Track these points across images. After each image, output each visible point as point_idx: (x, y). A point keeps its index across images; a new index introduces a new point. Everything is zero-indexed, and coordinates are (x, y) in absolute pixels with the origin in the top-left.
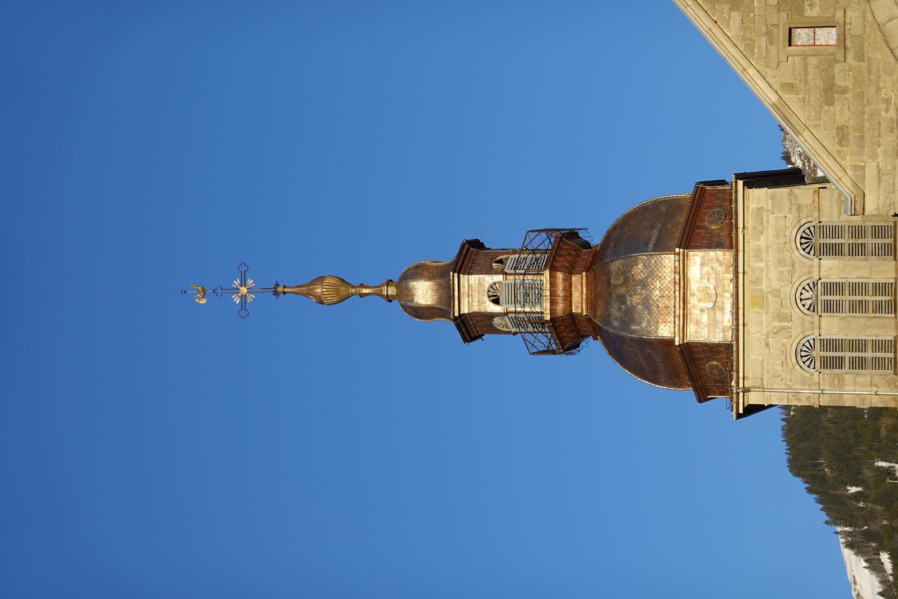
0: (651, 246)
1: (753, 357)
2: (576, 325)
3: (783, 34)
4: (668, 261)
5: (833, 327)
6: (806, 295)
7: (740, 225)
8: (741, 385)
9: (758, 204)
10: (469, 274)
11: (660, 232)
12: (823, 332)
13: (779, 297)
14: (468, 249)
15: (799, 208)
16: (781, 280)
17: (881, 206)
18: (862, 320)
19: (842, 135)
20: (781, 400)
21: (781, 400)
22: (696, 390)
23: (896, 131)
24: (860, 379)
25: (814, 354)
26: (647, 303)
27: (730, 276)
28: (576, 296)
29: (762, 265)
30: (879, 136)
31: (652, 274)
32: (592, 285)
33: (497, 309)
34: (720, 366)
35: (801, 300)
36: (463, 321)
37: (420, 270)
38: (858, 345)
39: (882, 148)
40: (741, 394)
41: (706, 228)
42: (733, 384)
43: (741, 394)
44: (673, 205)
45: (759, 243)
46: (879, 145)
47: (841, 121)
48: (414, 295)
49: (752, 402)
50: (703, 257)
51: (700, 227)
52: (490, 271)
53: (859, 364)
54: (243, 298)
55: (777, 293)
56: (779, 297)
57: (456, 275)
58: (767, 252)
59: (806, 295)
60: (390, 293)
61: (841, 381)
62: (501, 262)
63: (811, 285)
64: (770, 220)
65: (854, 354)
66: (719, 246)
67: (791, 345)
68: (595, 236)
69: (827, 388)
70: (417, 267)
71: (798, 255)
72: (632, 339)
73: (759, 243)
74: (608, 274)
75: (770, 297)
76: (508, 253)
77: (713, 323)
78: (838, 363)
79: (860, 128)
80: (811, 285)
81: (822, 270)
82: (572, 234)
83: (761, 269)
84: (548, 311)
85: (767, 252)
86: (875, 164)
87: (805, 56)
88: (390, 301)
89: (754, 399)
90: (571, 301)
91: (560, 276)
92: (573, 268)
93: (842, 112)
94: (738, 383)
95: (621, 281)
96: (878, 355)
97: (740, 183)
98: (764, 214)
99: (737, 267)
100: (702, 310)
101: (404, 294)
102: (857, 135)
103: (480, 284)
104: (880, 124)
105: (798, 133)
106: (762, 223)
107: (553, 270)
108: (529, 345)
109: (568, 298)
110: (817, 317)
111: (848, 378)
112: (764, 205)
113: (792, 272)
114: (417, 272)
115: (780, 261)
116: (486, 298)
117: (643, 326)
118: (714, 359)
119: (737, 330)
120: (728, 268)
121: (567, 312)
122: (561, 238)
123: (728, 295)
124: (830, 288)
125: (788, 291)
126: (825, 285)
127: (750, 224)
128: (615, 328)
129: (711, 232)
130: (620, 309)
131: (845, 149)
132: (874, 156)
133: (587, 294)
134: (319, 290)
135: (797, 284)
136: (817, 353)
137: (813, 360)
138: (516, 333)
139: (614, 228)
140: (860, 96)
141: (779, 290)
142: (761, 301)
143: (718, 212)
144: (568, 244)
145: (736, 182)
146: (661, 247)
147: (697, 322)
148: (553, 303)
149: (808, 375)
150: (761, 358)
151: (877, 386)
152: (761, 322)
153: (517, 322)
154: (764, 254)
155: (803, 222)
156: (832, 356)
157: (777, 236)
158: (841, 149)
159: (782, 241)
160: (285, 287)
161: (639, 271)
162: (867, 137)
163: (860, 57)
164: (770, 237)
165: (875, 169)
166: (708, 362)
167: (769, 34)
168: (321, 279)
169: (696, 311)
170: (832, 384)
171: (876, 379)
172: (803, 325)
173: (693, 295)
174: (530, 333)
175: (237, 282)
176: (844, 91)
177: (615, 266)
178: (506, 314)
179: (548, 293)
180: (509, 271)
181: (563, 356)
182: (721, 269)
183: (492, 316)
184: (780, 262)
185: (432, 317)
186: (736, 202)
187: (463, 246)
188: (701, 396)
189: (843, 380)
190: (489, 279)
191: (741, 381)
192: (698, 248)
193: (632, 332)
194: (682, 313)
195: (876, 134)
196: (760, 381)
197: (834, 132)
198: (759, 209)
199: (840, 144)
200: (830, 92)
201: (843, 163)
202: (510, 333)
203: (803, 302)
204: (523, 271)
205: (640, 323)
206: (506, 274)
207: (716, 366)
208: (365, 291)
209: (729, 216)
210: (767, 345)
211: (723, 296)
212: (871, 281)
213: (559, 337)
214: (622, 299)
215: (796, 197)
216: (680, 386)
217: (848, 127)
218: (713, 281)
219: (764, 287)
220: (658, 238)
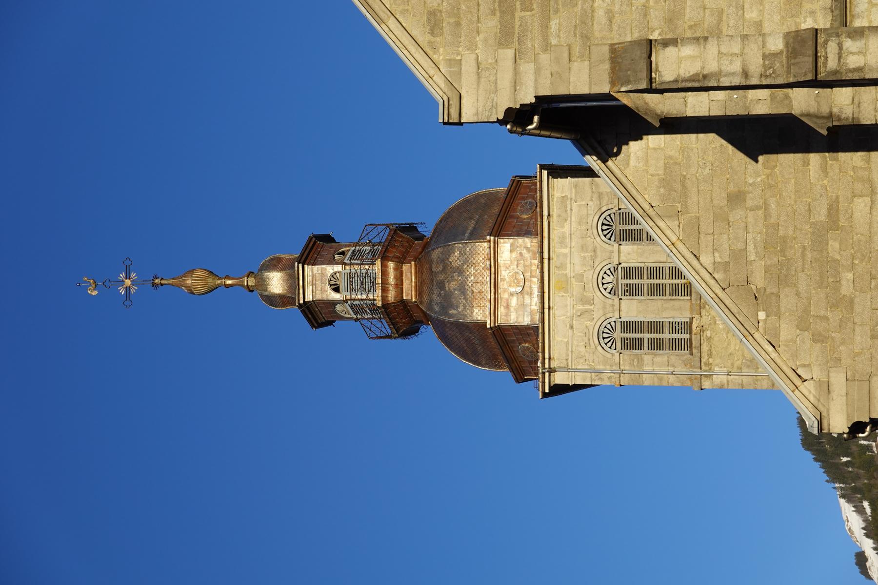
0: (467, 235)
1: (559, 339)
2: (408, 311)
4: (483, 247)
5: (633, 309)
6: (607, 279)
7: (545, 213)
8: (547, 366)
9: (562, 192)
10: (313, 264)
11: (477, 223)
12: (623, 314)
13: (582, 281)
14: (315, 243)
15: (600, 196)
16: (584, 265)
17: (480, 109)
18: (660, 303)
20: (584, 380)
21: (584, 380)
22: (512, 370)
23: (498, 14)
24: (658, 359)
25: (615, 335)
27: (536, 262)
28: (406, 285)
29: (566, 251)
30: (478, 21)
32: (419, 272)
33: (336, 296)
34: (532, 348)
35: (603, 284)
36: (308, 308)
37: (274, 262)
38: (656, 327)
39: (482, 36)
40: (547, 374)
41: (518, 217)
42: (539, 364)
43: (547, 374)
44: (491, 197)
45: (564, 230)
46: (478, 33)
48: (267, 285)
49: (557, 382)
50: (512, 245)
51: (512, 217)
52: (332, 262)
53: (657, 345)
54: (128, 289)
55: (580, 277)
56: (582, 281)
57: (300, 265)
58: (571, 238)
59: (607, 279)
60: (250, 284)
61: (641, 361)
62: (343, 253)
63: (612, 269)
64: (574, 208)
65: (653, 336)
66: (527, 233)
67: (593, 326)
68: (427, 230)
69: (627, 368)
70: (272, 260)
71: (599, 241)
72: (451, 323)
73: (564, 230)
74: (430, 262)
75: (573, 282)
76: (350, 246)
77: (523, 306)
78: (637, 344)
79: (455, 12)
80: (612, 269)
81: (622, 255)
82: (411, 229)
83: (565, 255)
84: (380, 298)
85: (571, 238)
86: (474, 56)
88: (252, 291)
89: (560, 378)
90: (402, 289)
91: (391, 265)
92: (404, 258)
94: (543, 363)
95: (441, 268)
96: (675, 336)
97: (545, 173)
98: (568, 203)
99: (542, 253)
100: (512, 294)
101: (262, 283)
102: (452, 20)
103: (323, 275)
104: (479, 5)
105: (380, 21)
106: (566, 211)
107: (384, 259)
108: (367, 330)
109: (399, 285)
110: (617, 300)
111: (647, 358)
112: (568, 194)
113: (594, 258)
114: (273, 264)
115: (582, 247)
116: (328, 286)
117: (460, 310)
118: (526, 342)
119: (543, 313)
120: (534, 254)
121: (399, 299)
122: (395, 230)
123: (535, 280)
124: (630, 272)
125: (590, 276)
126: (625, 269)
127: (555, 211)
128: (436, 313)
129: (522, 221)
130: (440, 295)
131: (438, 39)
132: (472, 47)
133: (416, 282)
134: (189, 282)
135: (599, 269)
136: (618, 335)
137: (614, 341)
138: (357, 320)
139: (441, 221)
141: (582, 275)
142: (566, 286)
143: (530, 203)
144: (402, 237)
145: (541, 172)
146: (476, 236)
147: (508, 307)
148: (384, 290)
149: (609, 356)
150: (566, 340)
151: (674, 366)
152: (566, 306)
154: (568, 240)
155: (604, 209)
156: (633, 337)
157: (580, 223)
158: (433, 40)
159: (584, 227)
160: (162, 279)
161: (455, 258)
162: (464, 22)
164: (574, 225)
165: (473, 64)
166: (520, 344)
168: (192, 271)
169: (506, 296)
170: (631, 365)
171: (673, 358)
172: (604, 308)
173: (503, 280)
174: (367, 319)
175: (122, 275)
177: (436, 254)
178: (346, 301)
179: (380, 281)
180: (348, 262)
181: (399, 340)
182: (527, 255)
183: (334, 303)
184: (583, 248)
185: (285, 304)
186: (541, 191)
187: (310, 239)
188: (518, 377)
189: (642, 360)
190: (330, 269)
191: (547, 361)
192: (508, 235)
193: (450, 316)
194: (493, 297)
195: (475, 19)
196: (565, 362)
197: (425, 18)
198: (563, 197)
199: (432, 34)
201: (435, 57)
202: (351, 319)
203: (605, 286)
204: (359, 262)
205: (457, 308)
206: (346, 264)
207: (528, 348)
208: (229, 282)
209: (536, 206)
210: (571, 327)
211: (531, 281)
212: (667, 265)
213: (393, 323)
214: (441, 285)
215: (597, 185)
216: (500, 367)
217: (441, 11)
218: (521, 268)
219: (568, 271)
220: (474, 228)
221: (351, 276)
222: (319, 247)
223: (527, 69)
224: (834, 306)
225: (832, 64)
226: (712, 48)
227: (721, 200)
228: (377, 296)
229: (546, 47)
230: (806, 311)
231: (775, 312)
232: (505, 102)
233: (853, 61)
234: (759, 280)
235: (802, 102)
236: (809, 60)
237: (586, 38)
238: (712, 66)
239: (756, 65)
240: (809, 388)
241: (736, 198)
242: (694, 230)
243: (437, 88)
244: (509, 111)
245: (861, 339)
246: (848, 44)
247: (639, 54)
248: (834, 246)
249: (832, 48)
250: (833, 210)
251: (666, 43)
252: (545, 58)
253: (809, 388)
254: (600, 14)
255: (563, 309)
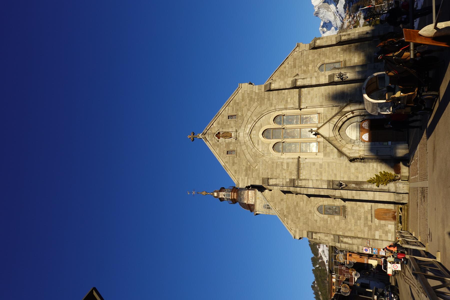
3: (226, 152)
4: (246, 192)
19: (235, 172)
26: (243, 198)
31: (244, 193)
47: (235, 169)
77: (252, 201)
79: (239, 170)
87: (229, 156)
89: (257, 213)
93: (236, 167)
101: (214, 194)
114: (215, 192)
132: (241, 176)
140: (239, 164)
142: (259, 198)
153: (228, 199)
163: (239, 157)
167: (223, 152)
176: (236, 163)
177: (239, 192)
190: (224, 193)
200: (234, 164)
221: (227, 194)
222: (222, 189)
223: (249, 180)
224: (297, 218)
225: (297, 184)
226: (278, 180)
227: (280, 200)
228: (230, 197)
229: (252, 177)
230: (293, 219)
231: (288, 219)
232: (246, 185)
233: (300, 184)
234: (285, 213)
235: (292, 189)
236: (293, 184)
237: (259, 176)
238: (278, 183)
239: (285, 183)
240: (293, 231)
241: (282, 200)
242: (275, 204)
243: (235, 182)
244: (246, 187)
245: (301, 224)
246: (299, 181)
247: (267, 180)
248: (297, 209)
249: (297, 182)
250: (297, 203)
251: (271, 179)
252: (252, 179)
253: (293, 231)
254: (261, 173)
255: (258, 202)
